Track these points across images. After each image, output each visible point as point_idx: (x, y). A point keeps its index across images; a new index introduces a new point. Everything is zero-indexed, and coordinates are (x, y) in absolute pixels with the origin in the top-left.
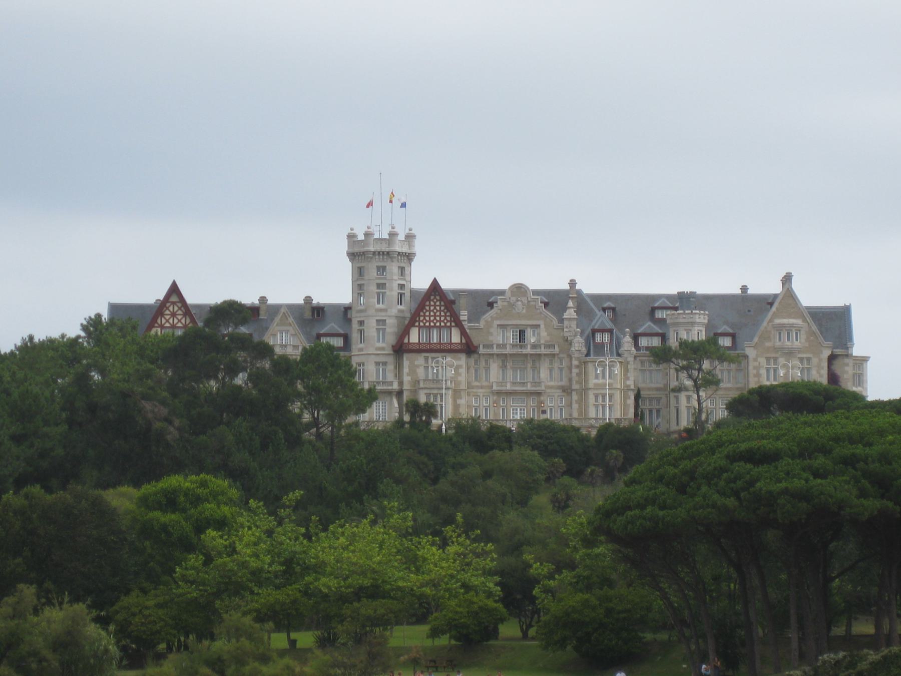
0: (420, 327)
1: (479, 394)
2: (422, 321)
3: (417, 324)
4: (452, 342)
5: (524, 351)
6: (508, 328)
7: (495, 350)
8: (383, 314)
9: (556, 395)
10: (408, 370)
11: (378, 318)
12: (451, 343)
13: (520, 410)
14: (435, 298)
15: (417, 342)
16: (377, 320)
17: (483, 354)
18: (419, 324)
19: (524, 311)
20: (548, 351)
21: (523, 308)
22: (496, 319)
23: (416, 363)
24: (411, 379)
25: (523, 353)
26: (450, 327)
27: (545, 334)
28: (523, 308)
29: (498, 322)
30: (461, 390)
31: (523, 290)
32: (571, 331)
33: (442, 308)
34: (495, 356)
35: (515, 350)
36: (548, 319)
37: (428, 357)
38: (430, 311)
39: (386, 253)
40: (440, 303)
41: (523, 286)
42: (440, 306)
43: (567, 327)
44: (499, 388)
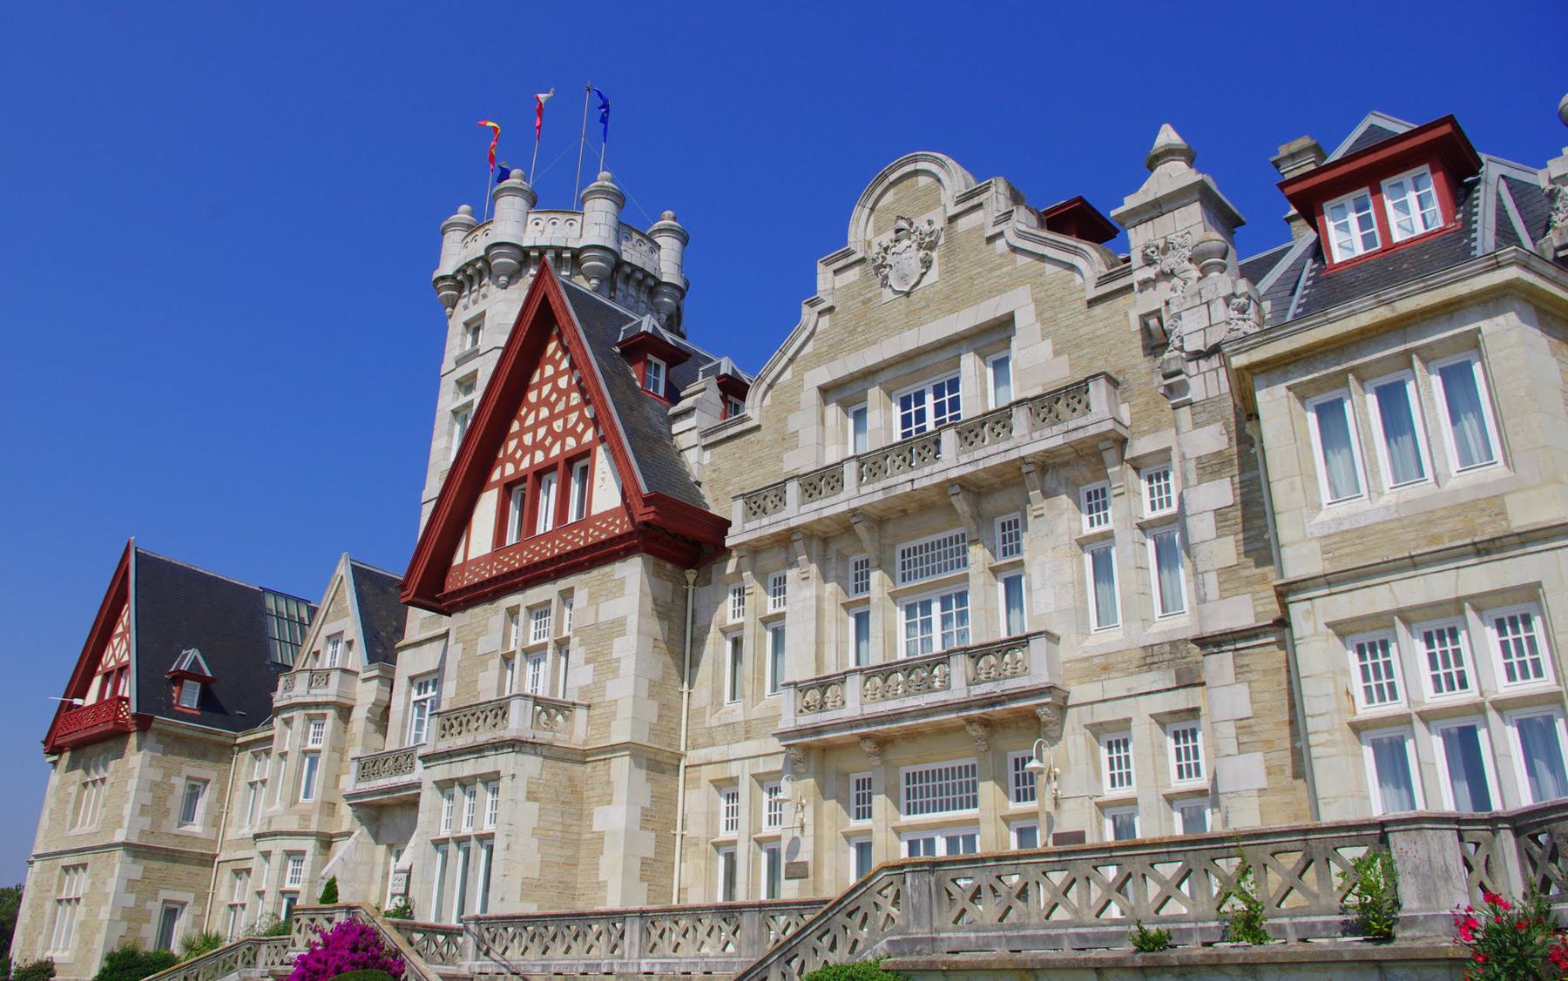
1: (734, 770)
2: (512, 458)
3: (496, 476)
4: (595, 511)
5: (926, 476)
7: (796, 512)
9: (1141, 713)
12: (585, 521)
17: (754, 550)
20: (1051, 439)
21: (927, 264)
22: (818, 359)
23: (479, 653)
25: (917, 485)
26: (587, 453)
27: (1047, 347)
28: (927, 264)
29: (825, 375)
30: (613, 749)
32: (1172, 274)
35: (878, 486)
36: (1050, 269)
38: (536, 407)
39: (479, 265)
41: (921, 165)
43: (1149, 262)
44: (808, 720)
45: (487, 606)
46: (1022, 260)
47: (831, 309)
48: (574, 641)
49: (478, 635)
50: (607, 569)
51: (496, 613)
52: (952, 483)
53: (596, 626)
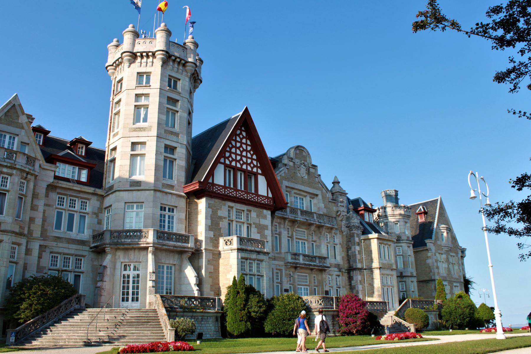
0: (226, 166)
6: (294, 191)
8: (174, 138)
10: (210, 221)
11: (168, 143)
13: (304, 288)
14: (241, 133)
15: (223, 184)
16: (165, 145)
18: (225, 161)
19: (306, 177)
24: (214, 236)
31: (304, 154)
33: (249, 148)
34: (287, 222)
37: (232, 207)
40: (246, 141)
41: (304, 150)
42: (246, 144)
45: (220, 201)
46: (320, 186)
47: (288, 169)
48: (253, 226)
49: (218, 209)
50: (261, 210)
51: (225, 205)
52: (316, 224)
53: (260, 224)
